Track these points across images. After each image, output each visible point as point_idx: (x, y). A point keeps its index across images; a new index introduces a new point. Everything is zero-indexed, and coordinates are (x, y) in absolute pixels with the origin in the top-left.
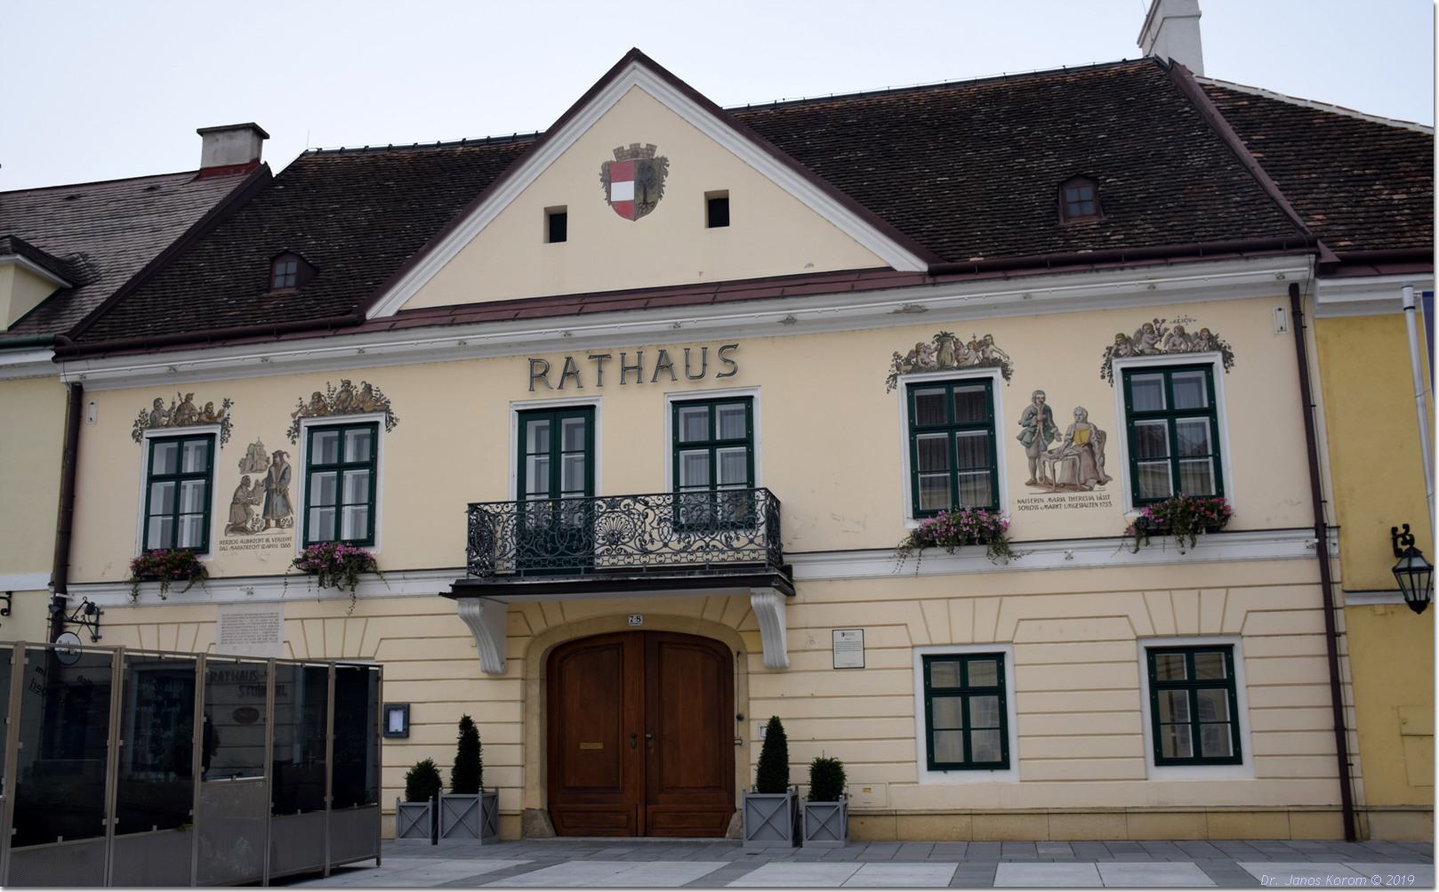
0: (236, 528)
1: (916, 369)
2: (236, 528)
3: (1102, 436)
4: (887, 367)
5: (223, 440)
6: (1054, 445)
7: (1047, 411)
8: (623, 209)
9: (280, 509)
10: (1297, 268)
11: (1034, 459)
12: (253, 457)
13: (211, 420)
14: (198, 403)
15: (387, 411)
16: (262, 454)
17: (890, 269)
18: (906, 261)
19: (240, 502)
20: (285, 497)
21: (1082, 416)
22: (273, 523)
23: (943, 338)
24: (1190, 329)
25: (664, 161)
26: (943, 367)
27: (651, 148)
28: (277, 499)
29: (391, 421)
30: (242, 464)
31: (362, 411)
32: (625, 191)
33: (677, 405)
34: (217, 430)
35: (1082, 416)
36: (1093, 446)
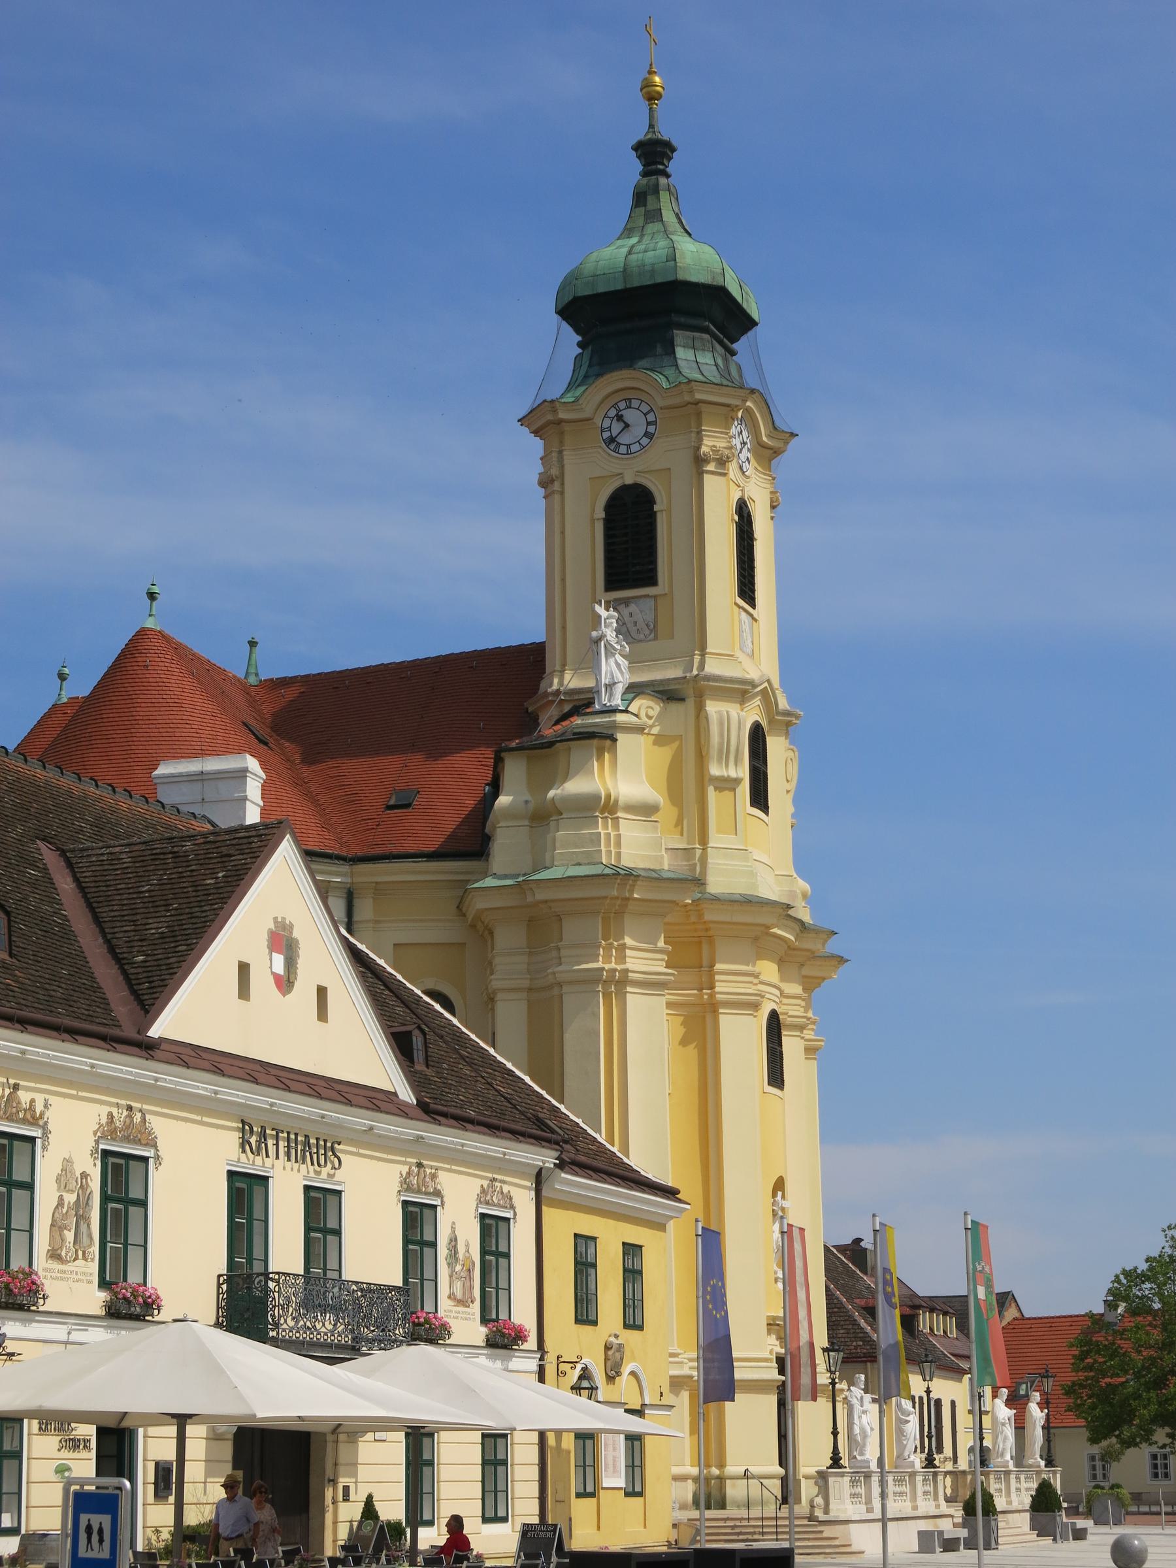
0: (54, 1255)
1: (409, 1189)
2: (54, 1255)
3: (473, 1263)
4: (396, 1187)
5: (44, 1148)
6: (458, 1268)
7: (456, 1240)
8: (277, 977)
9: (85, 1240)
10: (546, 1158)
11: (451, 1276)
14: (24, 1097)
15: (155, 1146)
16: (72, 1172)
18: (406, 1095)
19: (56, 1226)
20: (89, 1226)
21: (467, 1246)
22: (80, 1255)
24: (506, 1188)
25: (297, 941)
26: (419, 1191)
27: (291, 926)
28: (83, 1228)
29: (157, 1158)
30: (58, 1180)
32: (279, 963)
33: (307, 1188)
35: (467, 1246)
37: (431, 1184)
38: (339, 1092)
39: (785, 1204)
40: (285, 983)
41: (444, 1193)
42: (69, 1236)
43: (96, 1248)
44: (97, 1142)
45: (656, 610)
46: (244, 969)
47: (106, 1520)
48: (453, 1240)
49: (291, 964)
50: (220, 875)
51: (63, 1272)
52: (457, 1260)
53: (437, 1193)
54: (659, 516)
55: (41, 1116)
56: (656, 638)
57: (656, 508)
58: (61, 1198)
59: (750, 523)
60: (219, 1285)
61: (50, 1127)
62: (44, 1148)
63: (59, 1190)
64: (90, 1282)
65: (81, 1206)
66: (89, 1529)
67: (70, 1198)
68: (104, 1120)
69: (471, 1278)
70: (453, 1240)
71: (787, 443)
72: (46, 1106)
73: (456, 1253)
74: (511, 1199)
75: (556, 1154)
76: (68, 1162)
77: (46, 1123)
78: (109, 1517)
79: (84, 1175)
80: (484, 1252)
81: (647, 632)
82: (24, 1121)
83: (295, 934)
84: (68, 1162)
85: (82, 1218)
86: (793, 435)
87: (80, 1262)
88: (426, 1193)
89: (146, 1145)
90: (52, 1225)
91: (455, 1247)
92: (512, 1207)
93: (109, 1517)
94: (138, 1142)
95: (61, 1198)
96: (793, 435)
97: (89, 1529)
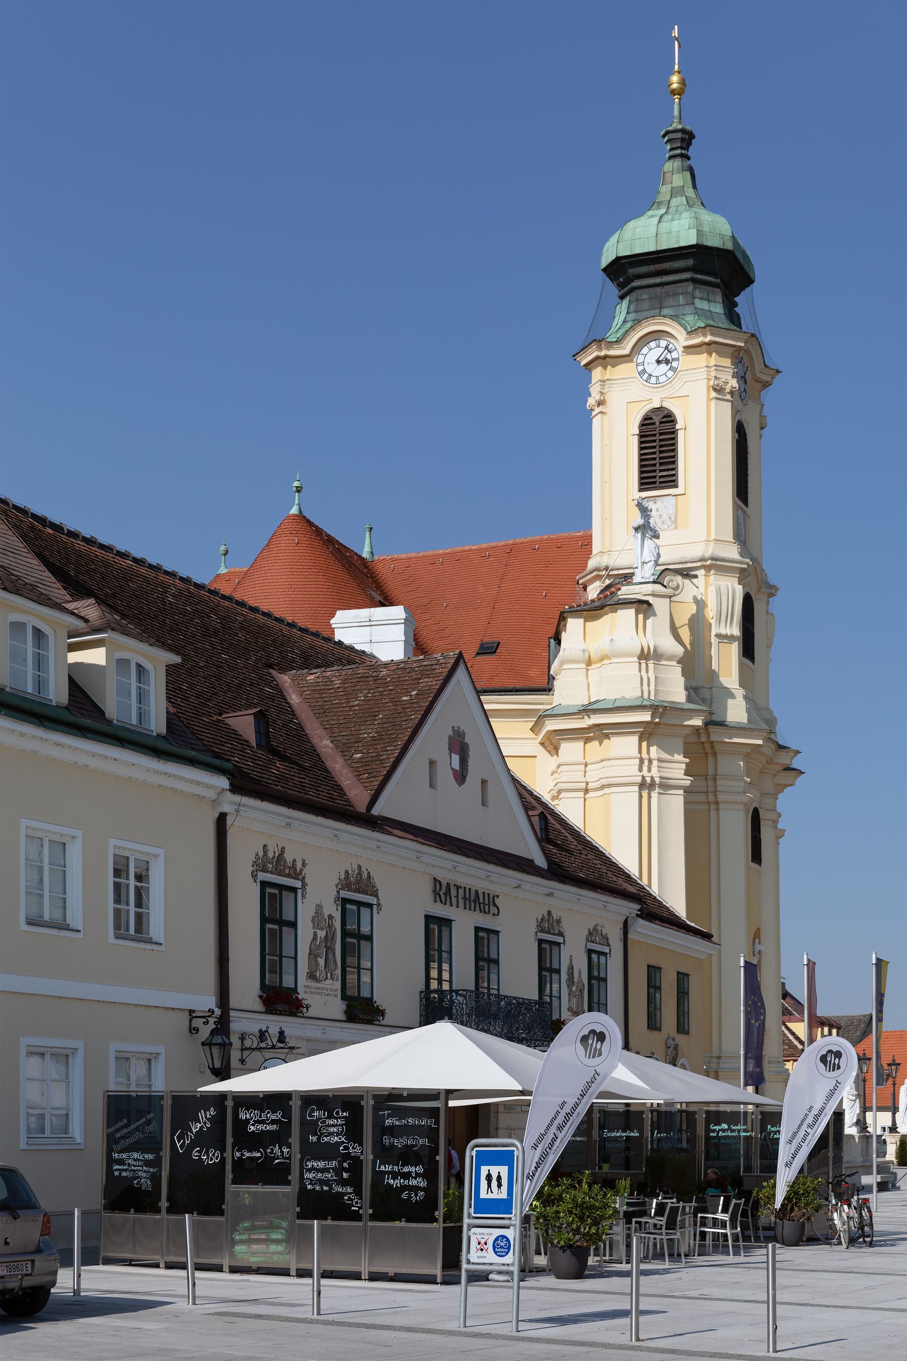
5: (303, 897)
9: (332, 965)
11: (569, 995)
12: (318, 917)
13: (296, 875)
15: (377, 896)
17: (532, 861)
18: (541, 861)
19: (313, 955)
20: (334, 954)
21: (580, 973)
23: (549, 913)
24: (604, 933)
26: (549, 933)
27: (464, 733)
28: (330, 956)
29: (379, 905)
31: (366, 893)
34: (298, 884)
35: (580, 973)
36: (581, 991)
37: (557, 927)
38: (498, 859)
39: (762, 948)
40: (461, 776)
41: (566, 934)
42: (321, 961)
43: (339, 971)
44: (338, 892)
45: (677, 506)
46: (432, 763)
47: (504, 1170)
48: (571, 968)
49: (464, 761)
50: (414, 693)
51: (318, 988)
52: (573, 983)
53: (561, 934)
54: (681, 434)
55: (301, 871)
56: (676, 528)
57: (678, 427)
58: (315, 934)
59: (746, 440)
60: (421, 1000)
61: (307, 880)
62: (303, 897)
63: (313, 928)
64: (336, 996)
65: (329, 939)
66: (489, 1177)
67: (322, 934)
68: (343, 877)
69: (582, 997)
70: (571, 968)
71: (773, 378)
72: (304, 865)
73: (573, 978)
74: (608, 939)
75: (638, 907)
76: (319, 907)
77: (304, 878)
78: (507, 1167)
79: (331, 917)
80: (590, 977)
81: (670, 523)
82: (289, 876)
83: (466, 740)
84: (319, 907)
85: (330, 949)
86: (778, 371)
87: (329, 981)
88: (554, 934)
89: (371, 895)
90: (310, 954)
91: (572, 973)
92: (608, 945)
93: (507, 1167)
94: (365, 893)
95: (315, 934)
96: (778, 371)
97: (489, 1177)
